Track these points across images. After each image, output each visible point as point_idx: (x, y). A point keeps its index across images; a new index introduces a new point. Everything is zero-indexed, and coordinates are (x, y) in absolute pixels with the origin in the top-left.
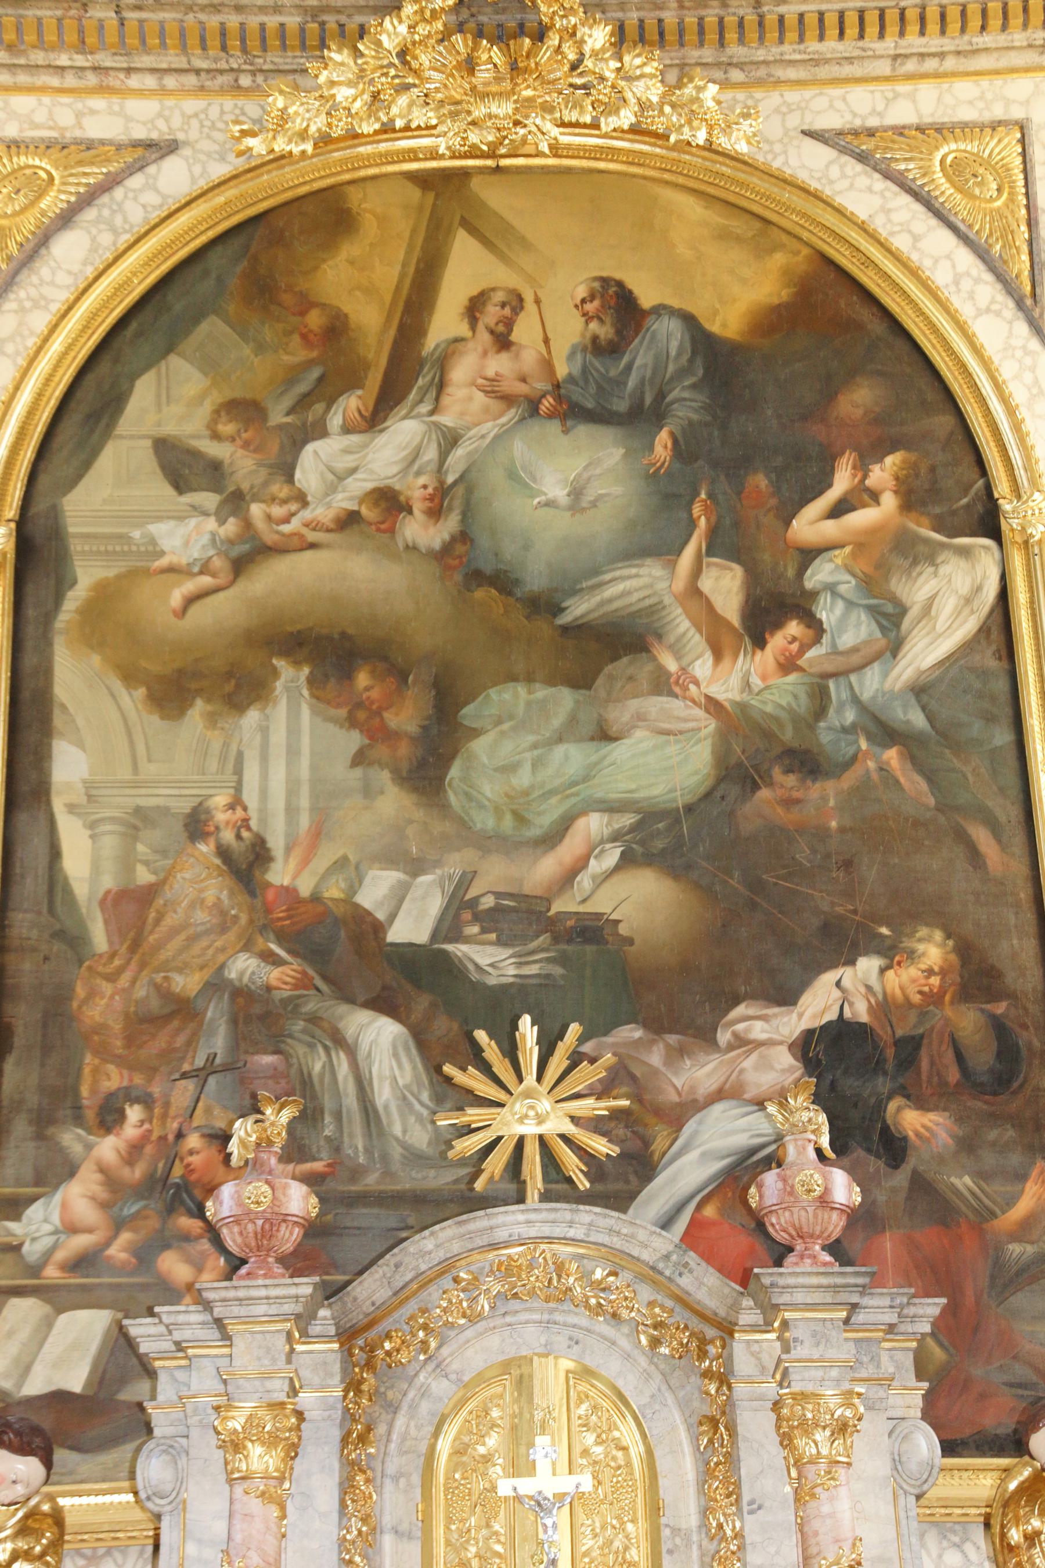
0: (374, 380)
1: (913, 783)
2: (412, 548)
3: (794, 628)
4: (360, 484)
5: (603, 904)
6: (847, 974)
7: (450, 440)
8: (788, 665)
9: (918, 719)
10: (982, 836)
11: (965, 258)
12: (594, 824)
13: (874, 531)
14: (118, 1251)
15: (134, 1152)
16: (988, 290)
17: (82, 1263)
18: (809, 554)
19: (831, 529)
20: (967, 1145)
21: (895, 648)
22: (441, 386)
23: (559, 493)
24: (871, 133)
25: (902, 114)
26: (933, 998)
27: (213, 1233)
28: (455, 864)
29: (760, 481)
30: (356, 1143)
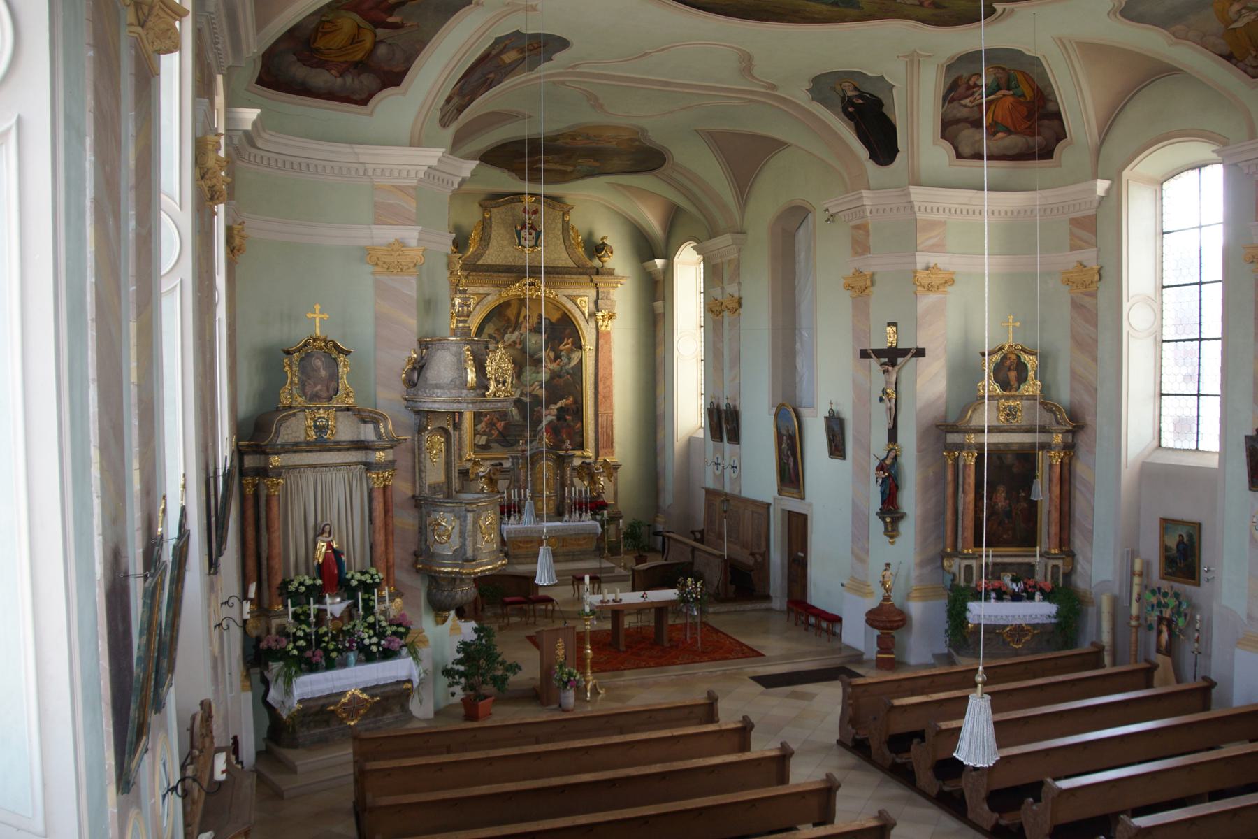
0: (514, 325)
1: (570, 379)
2: (517, 349)
3: (559, 360)
4: (512, 340)
5: (537, 393)
6: (562, 401)
7: (522, 335)
8: (558, 365)
9: (571, 371)
10: (578, 386)
11: (580, 313)
12: (536, 383)
13: (568, 348)
14: (487, 430)
15: (488, 420)
16: (583, 318)
17: (484, 431)
18: (562, 350)
19: (564, 348)
20: (573, 420)
21: (570, 363)
22: (520, 327)
23: (534, 342)
24: (571, 296)
25: (575, 294)
26: (570, 404)
27: (498, 429)
28: (522, 388)
29: (556, 342)
30: (511, 419)
